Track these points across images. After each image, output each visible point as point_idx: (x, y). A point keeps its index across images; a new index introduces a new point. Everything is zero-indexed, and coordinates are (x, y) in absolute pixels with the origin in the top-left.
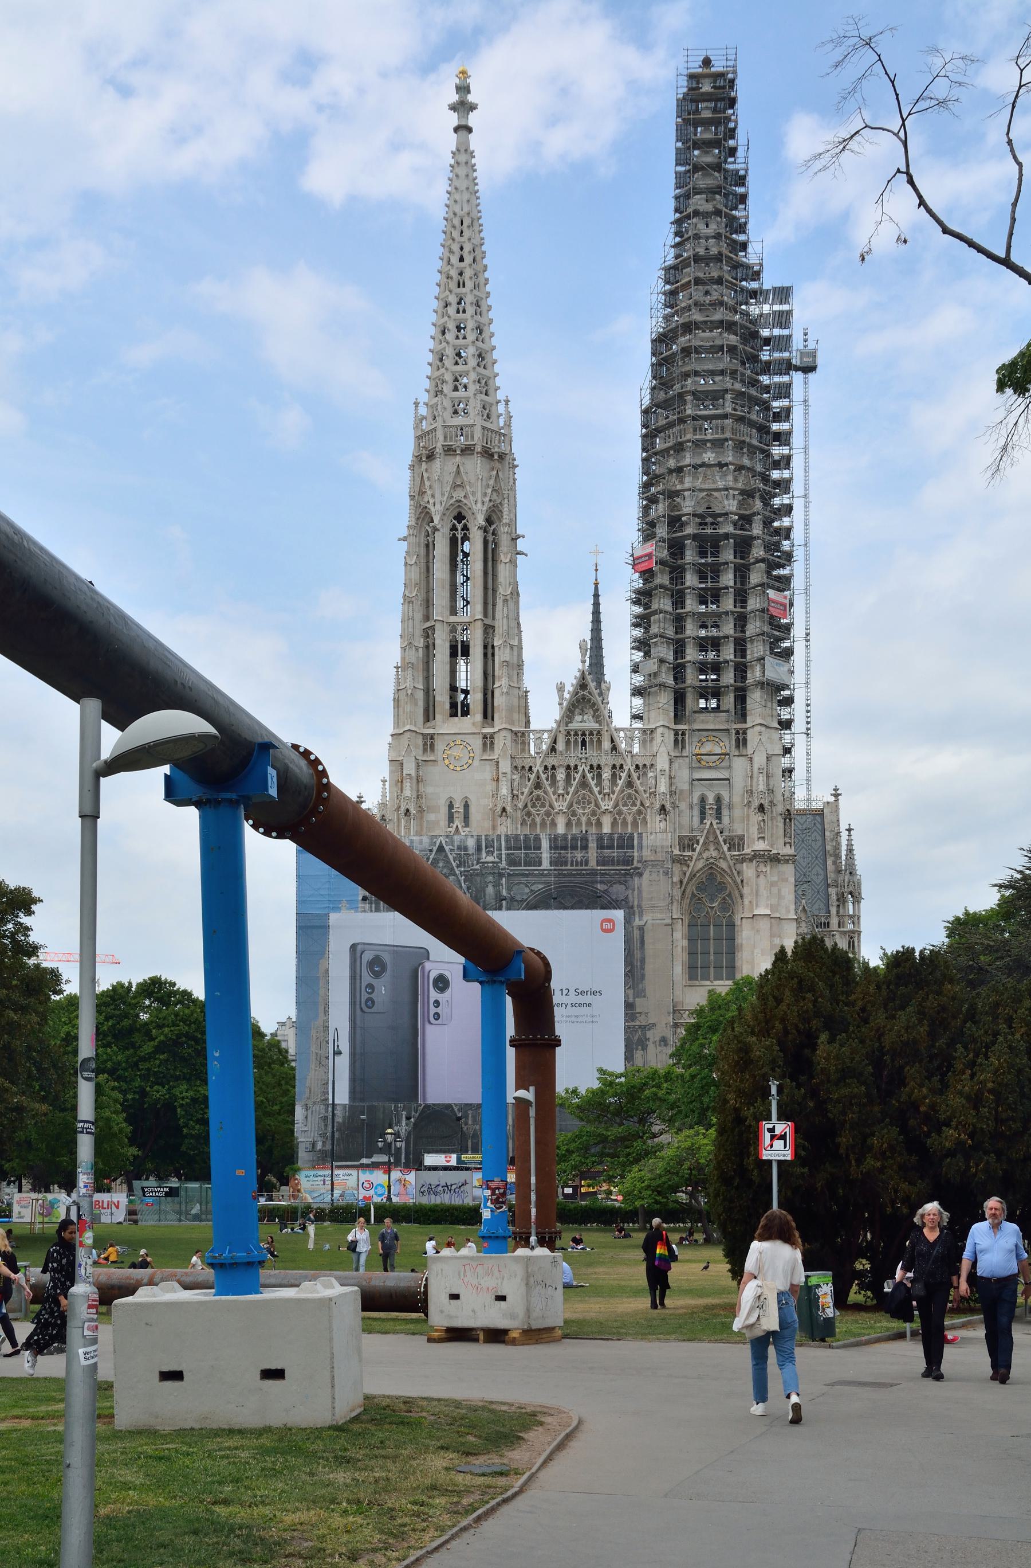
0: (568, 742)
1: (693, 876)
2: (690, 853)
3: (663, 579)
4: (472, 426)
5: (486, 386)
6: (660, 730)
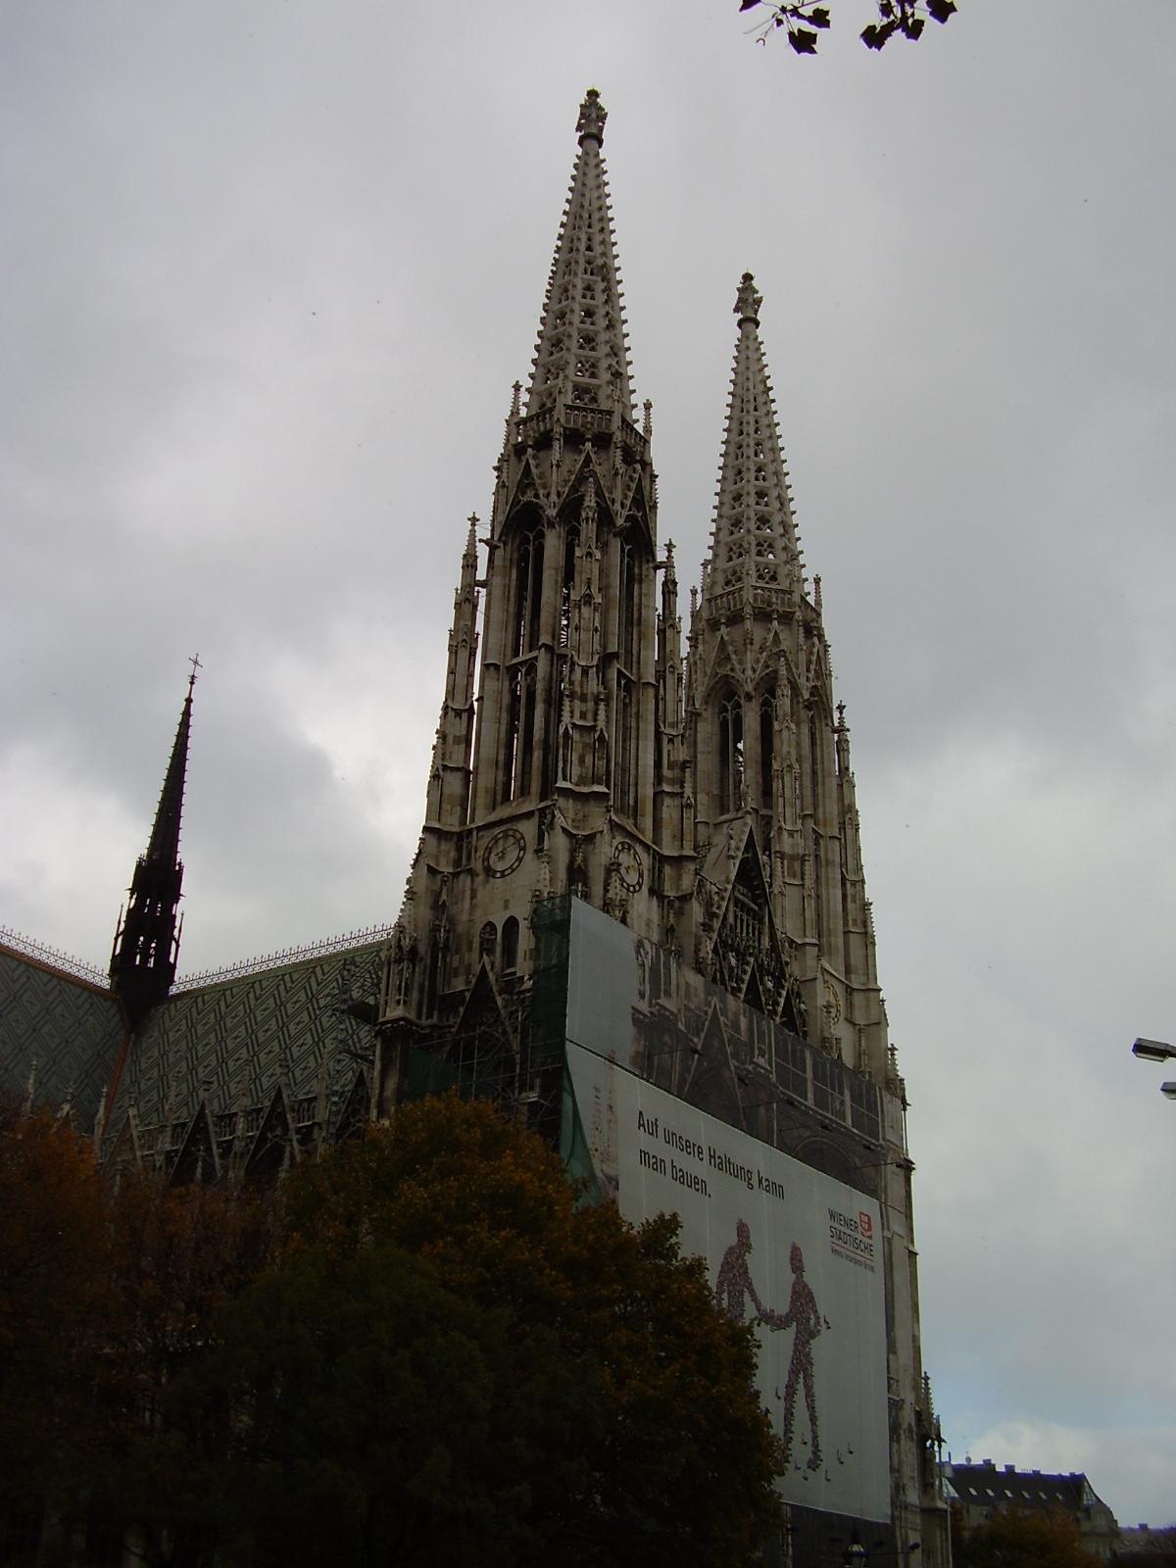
0: (736, 917)
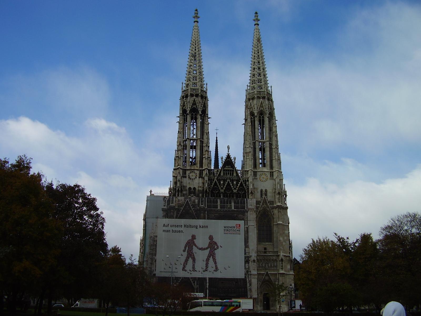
0: (224, 173)
1: (259, 212)
2: (258, 206)
4: (198, 89)
5: (201, 80)
6: (250, 171)
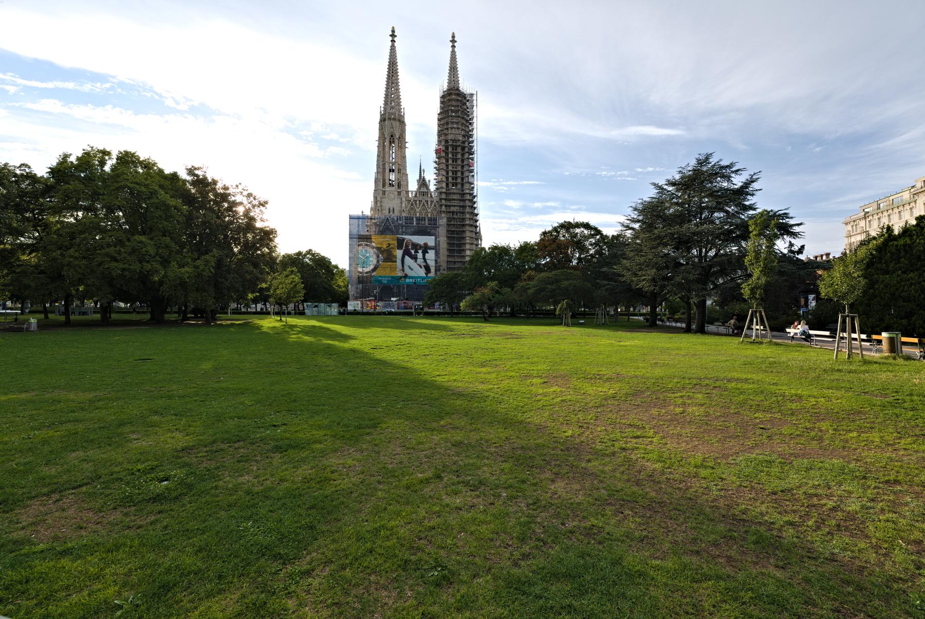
3: (443, 154)
